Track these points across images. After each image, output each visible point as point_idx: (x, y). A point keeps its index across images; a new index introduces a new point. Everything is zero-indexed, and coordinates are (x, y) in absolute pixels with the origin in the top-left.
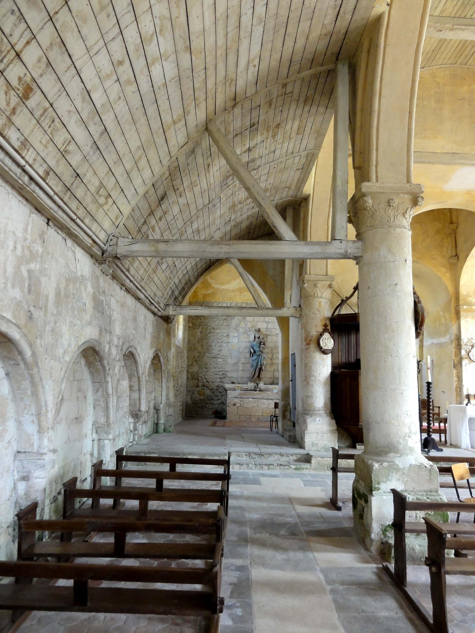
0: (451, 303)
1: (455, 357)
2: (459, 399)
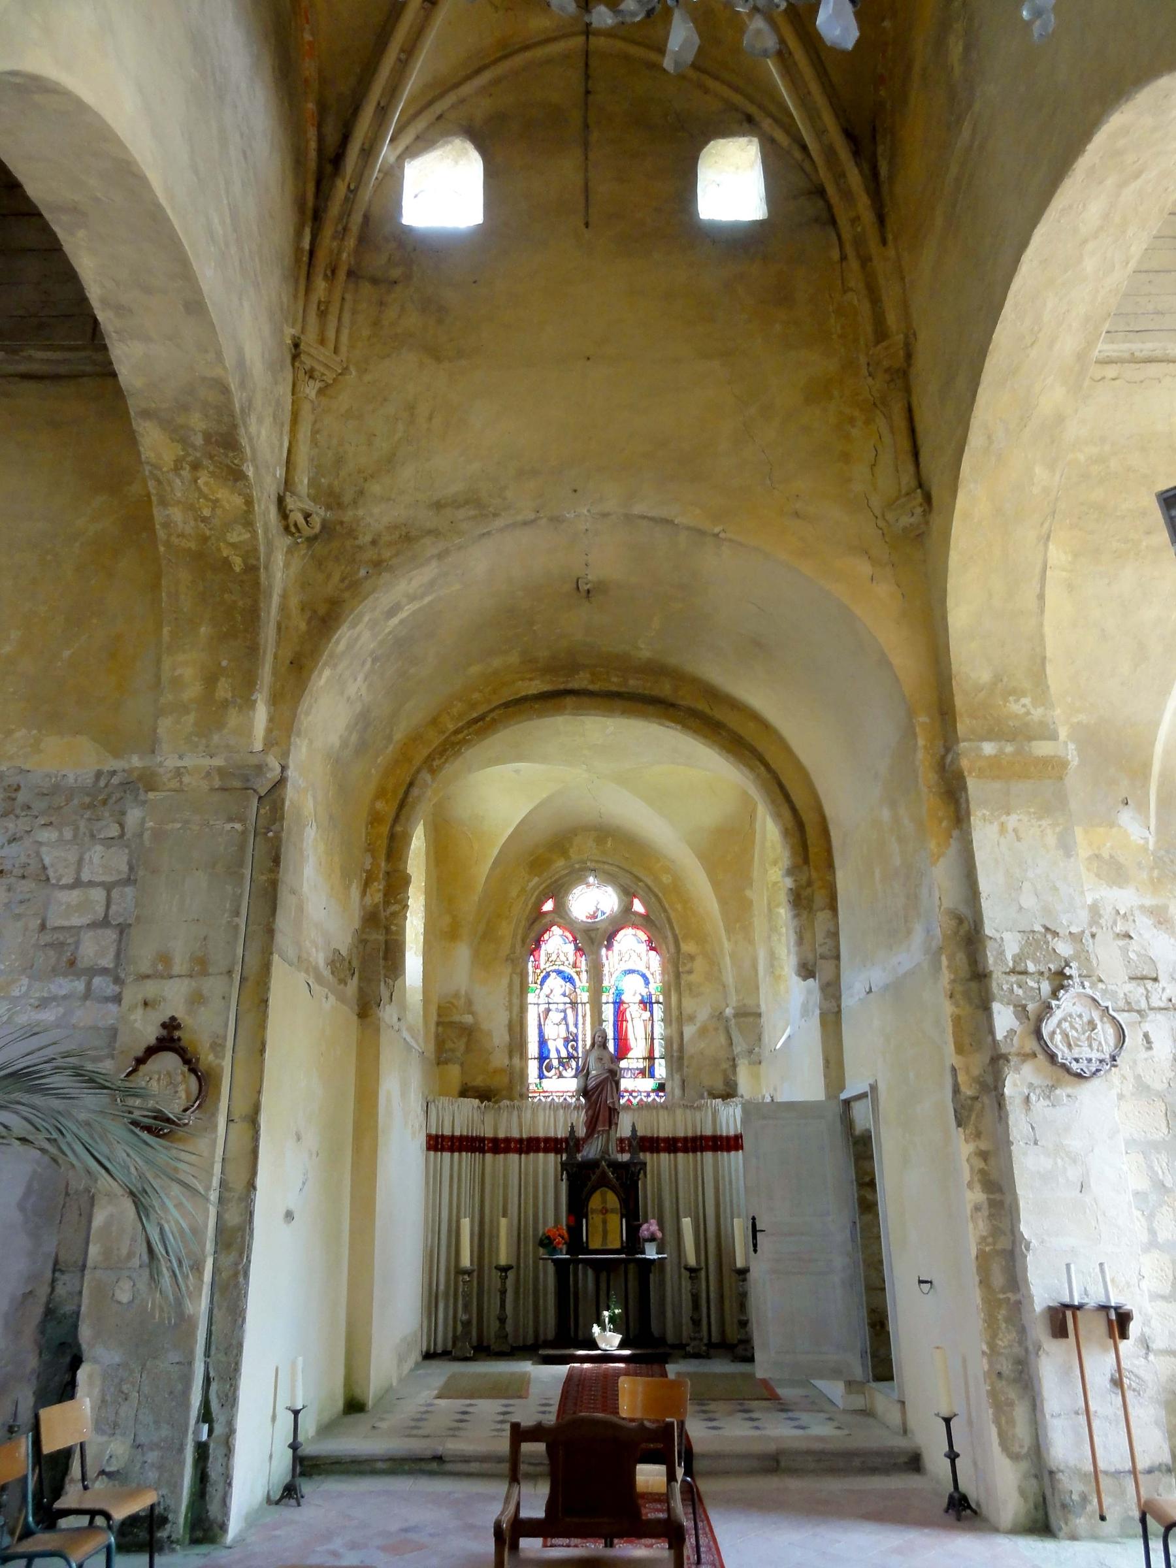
0: (915, 735)
1: (960, 1050)
2: (1006, 1339)
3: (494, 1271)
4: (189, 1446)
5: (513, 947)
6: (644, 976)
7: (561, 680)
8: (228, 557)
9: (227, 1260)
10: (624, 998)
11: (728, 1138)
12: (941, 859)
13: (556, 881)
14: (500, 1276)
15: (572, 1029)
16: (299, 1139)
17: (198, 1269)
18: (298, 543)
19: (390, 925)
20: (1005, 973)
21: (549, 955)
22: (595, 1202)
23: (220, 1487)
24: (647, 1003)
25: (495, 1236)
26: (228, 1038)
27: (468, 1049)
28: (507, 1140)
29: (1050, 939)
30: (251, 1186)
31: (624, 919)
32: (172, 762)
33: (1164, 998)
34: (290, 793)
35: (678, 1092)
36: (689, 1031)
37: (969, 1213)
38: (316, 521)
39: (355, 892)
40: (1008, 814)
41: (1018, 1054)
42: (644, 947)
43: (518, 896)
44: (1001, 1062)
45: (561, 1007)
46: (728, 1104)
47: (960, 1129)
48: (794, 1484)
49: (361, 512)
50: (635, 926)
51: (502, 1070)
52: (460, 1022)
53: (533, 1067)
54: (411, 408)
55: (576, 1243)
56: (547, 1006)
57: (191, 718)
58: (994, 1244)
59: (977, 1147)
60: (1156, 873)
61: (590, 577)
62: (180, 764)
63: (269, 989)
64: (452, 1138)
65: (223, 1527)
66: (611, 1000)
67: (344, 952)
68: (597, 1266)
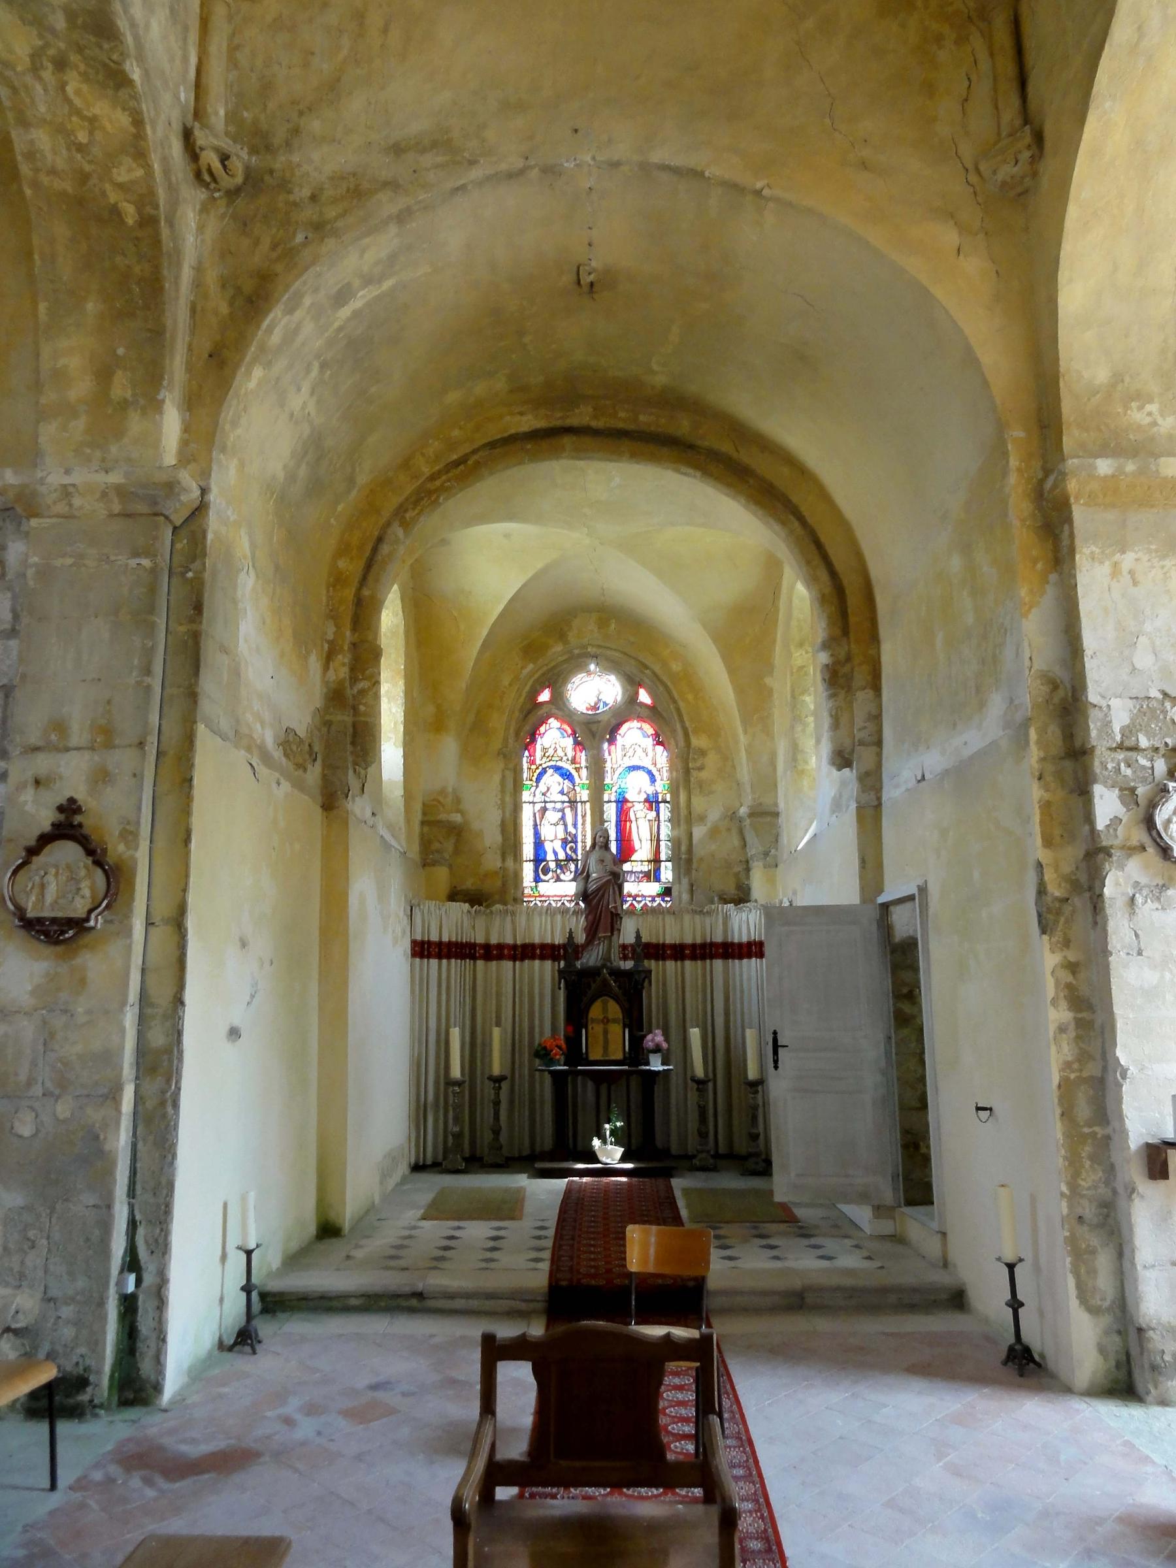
0: (1005, 454)
1: (1048, 842)
2: (1090, 1178)
3: (487, 1081)
4: (111, 1299)
5: (506, 740)
6: (650, 773)
7: (559, 415)
8: (116, 203)
9: (152, 1087)
10: (629, 796)
11: (740, 945)
12: (1034, 610)
13: (554, 667)
14: (494, 1088)
15: (571, 829)
16: (244, 944)
17: (114, 1098)
18: (214, 199)
19: (359, 705)
20: (1110, 749)
21: (545, 750)
22: (596, 1011)
23: (152, 1343)
24: (652, 802)
25: (487, 1045)
26: (143, 821)
27: (457, 852)
28: (500, 947)
29: (1169, 708)
30: (179, 1001)
31: (628, 710)
32: (56, 478)
34: (214, 524)
35: (685, 897)
36: (699, 832)
37: (1051, 1034)
38: (237, 166)
39: (315, 663)
40: (1124, 552)
41: (1123, 848)
42: (650, 742)
43: (510, 685)
44: (1101, 856)
45: (559, 806)
46: (741, 909)
47: (1045, 937)
48: (822, 1324)
49: (296, 158)
50: (640, 719)
51: (496, 873)
52: (448, 822)
53: (528, 870)
54: (360, 17)
55: (574, 1053)
56: (543, 805)
57: (79, 425)
58: (1081, 1071)
59: (1065, 957)
61: (594, 264)
62: (67, 480)
63: (193, 765)
64: (440, 944)
65: (158, 1388)
66: (613, 799)
67: (302, 733)
68: (598, 1077)
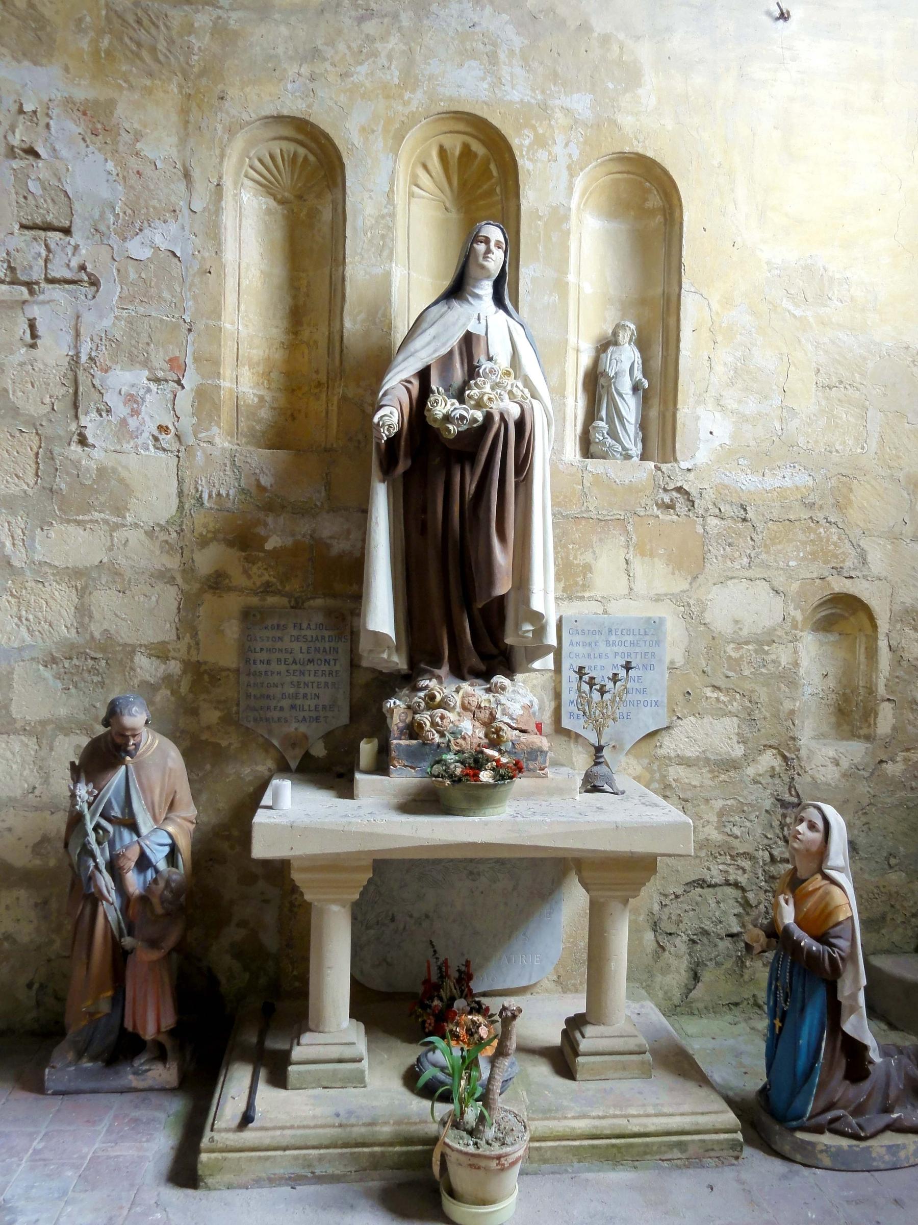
33: (74, 263)
60: (105, 43)
